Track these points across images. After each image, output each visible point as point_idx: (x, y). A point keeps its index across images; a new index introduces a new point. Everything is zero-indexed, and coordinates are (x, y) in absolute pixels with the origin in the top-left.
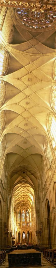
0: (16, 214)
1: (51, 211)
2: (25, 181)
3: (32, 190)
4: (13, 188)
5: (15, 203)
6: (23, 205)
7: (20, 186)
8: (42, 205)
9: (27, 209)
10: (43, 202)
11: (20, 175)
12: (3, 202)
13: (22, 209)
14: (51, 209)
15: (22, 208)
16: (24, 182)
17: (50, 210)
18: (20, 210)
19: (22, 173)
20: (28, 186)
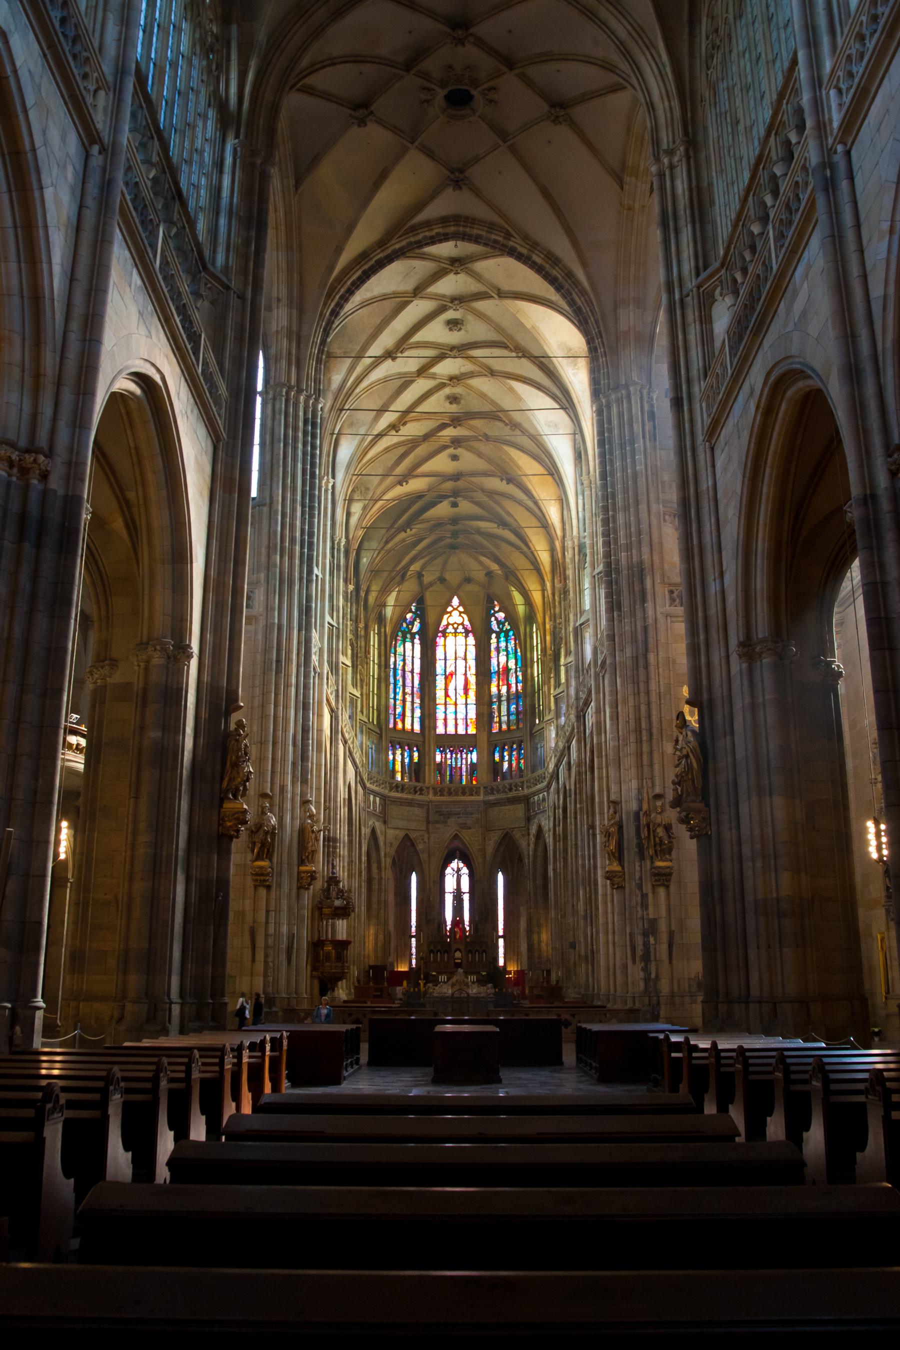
0: (374, 640)
1: (869, 499)
2: (470, 221)
4: (335, 313)
5: (357, 508)
6: (455, 534)
7: (418, 292)
8: (706, 483)
11: (410, 135)
13: (438, 587)
15: (442, 580)
16: (455, 236)
17: (855, 491)
18: (421, 601)
19: (441, 93)
20: (506, 287)
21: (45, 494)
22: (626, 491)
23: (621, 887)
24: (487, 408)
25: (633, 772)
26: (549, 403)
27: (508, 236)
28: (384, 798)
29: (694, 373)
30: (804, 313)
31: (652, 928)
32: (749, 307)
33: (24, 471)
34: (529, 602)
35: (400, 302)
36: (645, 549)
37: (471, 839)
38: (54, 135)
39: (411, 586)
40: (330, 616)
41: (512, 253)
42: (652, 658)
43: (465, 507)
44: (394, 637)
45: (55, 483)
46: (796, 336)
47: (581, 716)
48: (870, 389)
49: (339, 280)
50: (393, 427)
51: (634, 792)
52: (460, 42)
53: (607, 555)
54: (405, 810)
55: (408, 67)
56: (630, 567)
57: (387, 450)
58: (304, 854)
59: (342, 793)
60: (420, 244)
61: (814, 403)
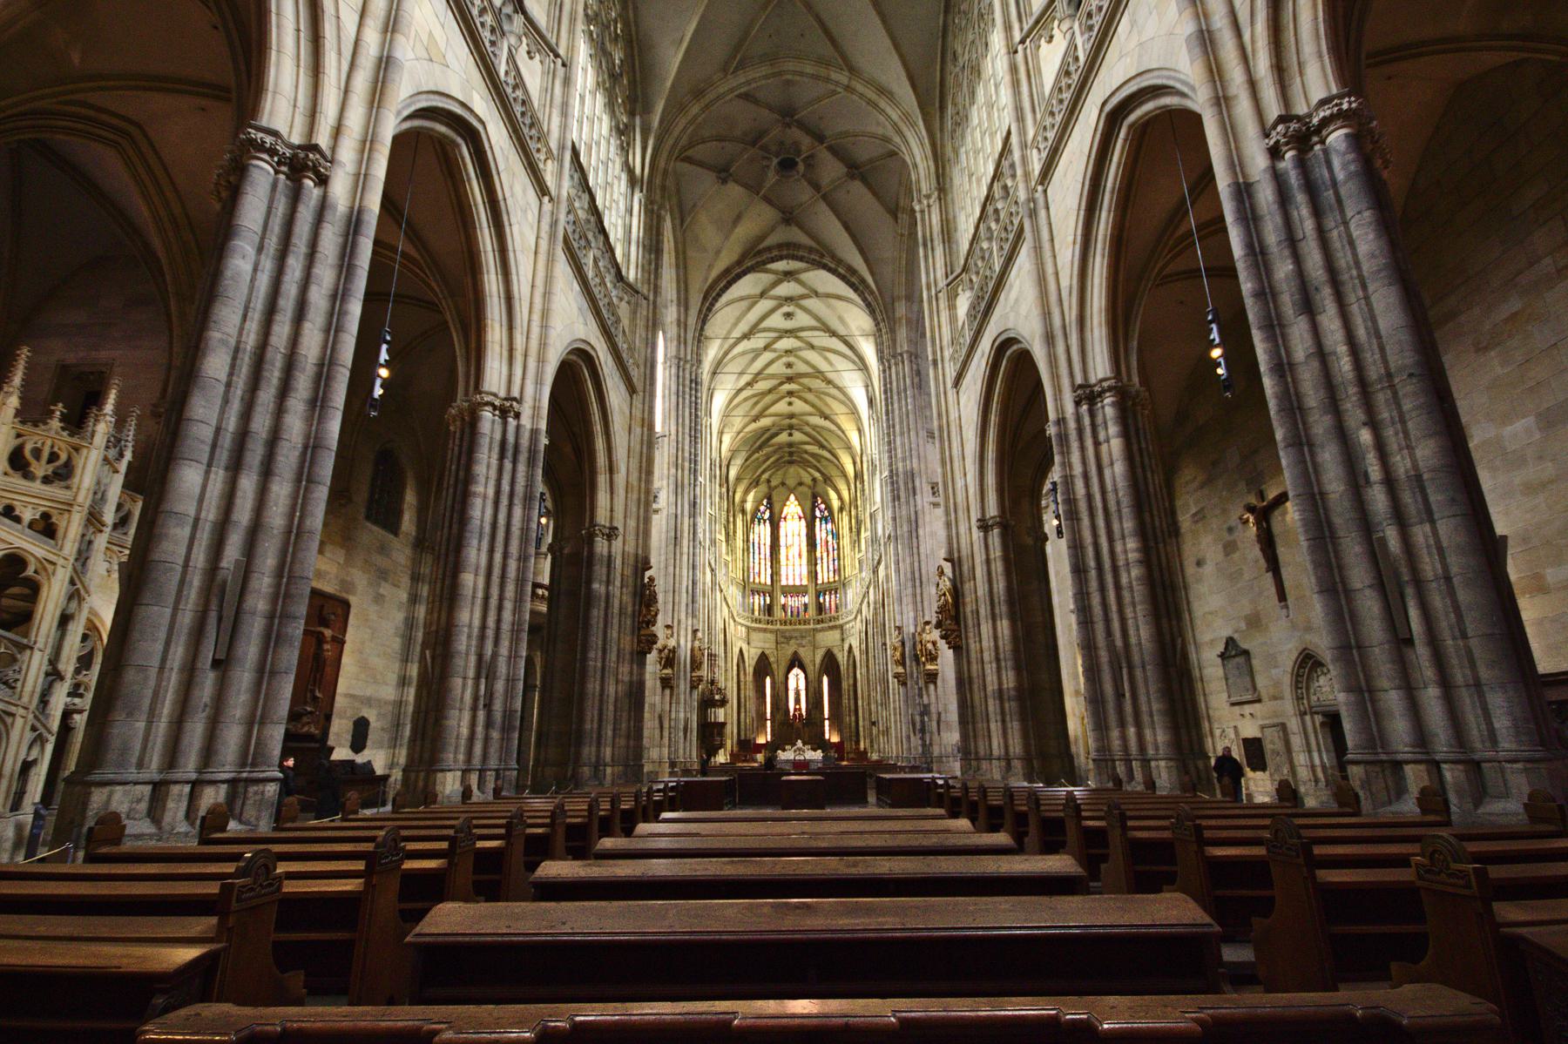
1: (1061, 421)
3: (857, 320)
4: (709, 310)
5: (727, 439)
6: (791, 454)
7: (762, 295)
8: (953, 415)
9: (819, 489)
10: (957, 382)
12: (623, 388)
13: (781, 489)
14: (1059, 403)
15: (783, 484)
16: (787, 257)
17: (1052, 415)
18: (769, 498)
19: (775, 161)
20: (821, 290)
21: (518, 427)
22: (901, 422)
23: (904, 684)
24: (810, 370)
25: (911, 607)
26: (851, 366)
27: (822, 256)
28: (748, 628)
29: (945, 343)
30: (1017, 300)
31: (925, 711)
32: (979, 298)
33: (504, 412)
34: (840, 498)
35: (753, 300)
36: (915, 461)
37: (805, 654)
38: (518, 189)
39: (763, 488)
40: (711, 506)
41: (825, 267)
42: (921, 532)
43: (798, 436)
44: (753, 521)
45: (526, 421)
46: (1012, 315)
47: (875, 571)
48: (1061, 349)
49: (711, 287)
50: (749, 384)
51: (911, 621)
52: (789, 126)
53: (891, 465)
54: (761, 635)
55: (754, 143)
56: (905, 473)
57: (746, 400)
58: (696, 664)
59: (720, 625)
60: (764, 263)
61: (1024, 360)
